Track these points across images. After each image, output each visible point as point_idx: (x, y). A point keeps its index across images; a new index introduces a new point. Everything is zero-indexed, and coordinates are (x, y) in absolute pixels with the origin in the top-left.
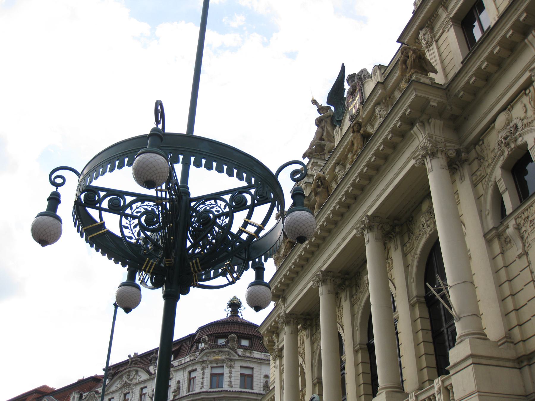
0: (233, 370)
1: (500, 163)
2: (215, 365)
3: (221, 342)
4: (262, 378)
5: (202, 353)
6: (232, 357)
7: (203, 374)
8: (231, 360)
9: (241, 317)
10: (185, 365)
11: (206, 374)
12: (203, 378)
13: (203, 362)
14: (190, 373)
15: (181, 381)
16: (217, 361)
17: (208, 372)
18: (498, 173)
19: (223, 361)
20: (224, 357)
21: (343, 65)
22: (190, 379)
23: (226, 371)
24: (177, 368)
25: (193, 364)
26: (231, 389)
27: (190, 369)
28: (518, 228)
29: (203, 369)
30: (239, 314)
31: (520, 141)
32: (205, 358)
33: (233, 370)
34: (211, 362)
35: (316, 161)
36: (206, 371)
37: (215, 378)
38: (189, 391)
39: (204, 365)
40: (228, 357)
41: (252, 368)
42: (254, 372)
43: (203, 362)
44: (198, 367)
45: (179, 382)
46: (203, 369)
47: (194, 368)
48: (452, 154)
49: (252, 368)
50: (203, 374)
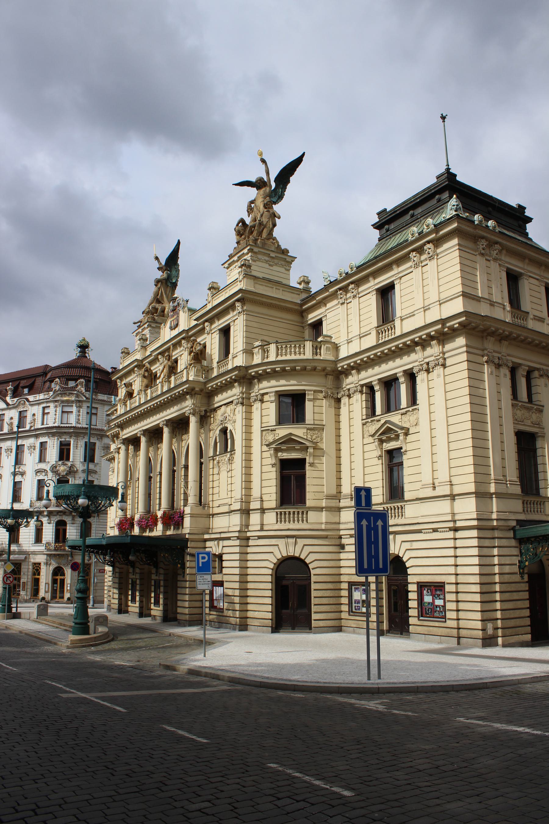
0: (81, 410)
1: (219, 428)
2: (66, 404)
3: (71, 384)
4: (105, 417)
5: (56, 394)
6: (80, 399)
7: (56, 411)
8: (80, 401)
9: (88, 358)
10: (40, 402)
11: (58, 411)
12: (56, 415)
13: (56, 401)
14: (44, 408)
15: (36, 414)
16: (68, 401)
17: (59, 410)
18: (218, 432)
19: (73, 402)
20: (73, 398)
21: (179, 241)
22: (44, 414)
23: (74, 409)
24: (32, 403)
25: (47, 402)
26: (79, 426)
27: (44, 405)
28: (218, 463)
29: (56, 407)
30: (87, 355)
31: (226, 425)
32: (58, 398)
33: (81, 410)
34: (63, 402)
35: (151, 324)
36: (58, 409)
37: (65, 415)
38: (43, 424)
39: (57, 404)
40: (77, 399)
41: (97, 408)
42: (98, 412)
43: (56, 401)
44: (52, 405)
45: (34, 415)
46: (56, 407)
47: (48, 405)
48: (203, 413)
49: (97, 408)
50: (56, 411)
